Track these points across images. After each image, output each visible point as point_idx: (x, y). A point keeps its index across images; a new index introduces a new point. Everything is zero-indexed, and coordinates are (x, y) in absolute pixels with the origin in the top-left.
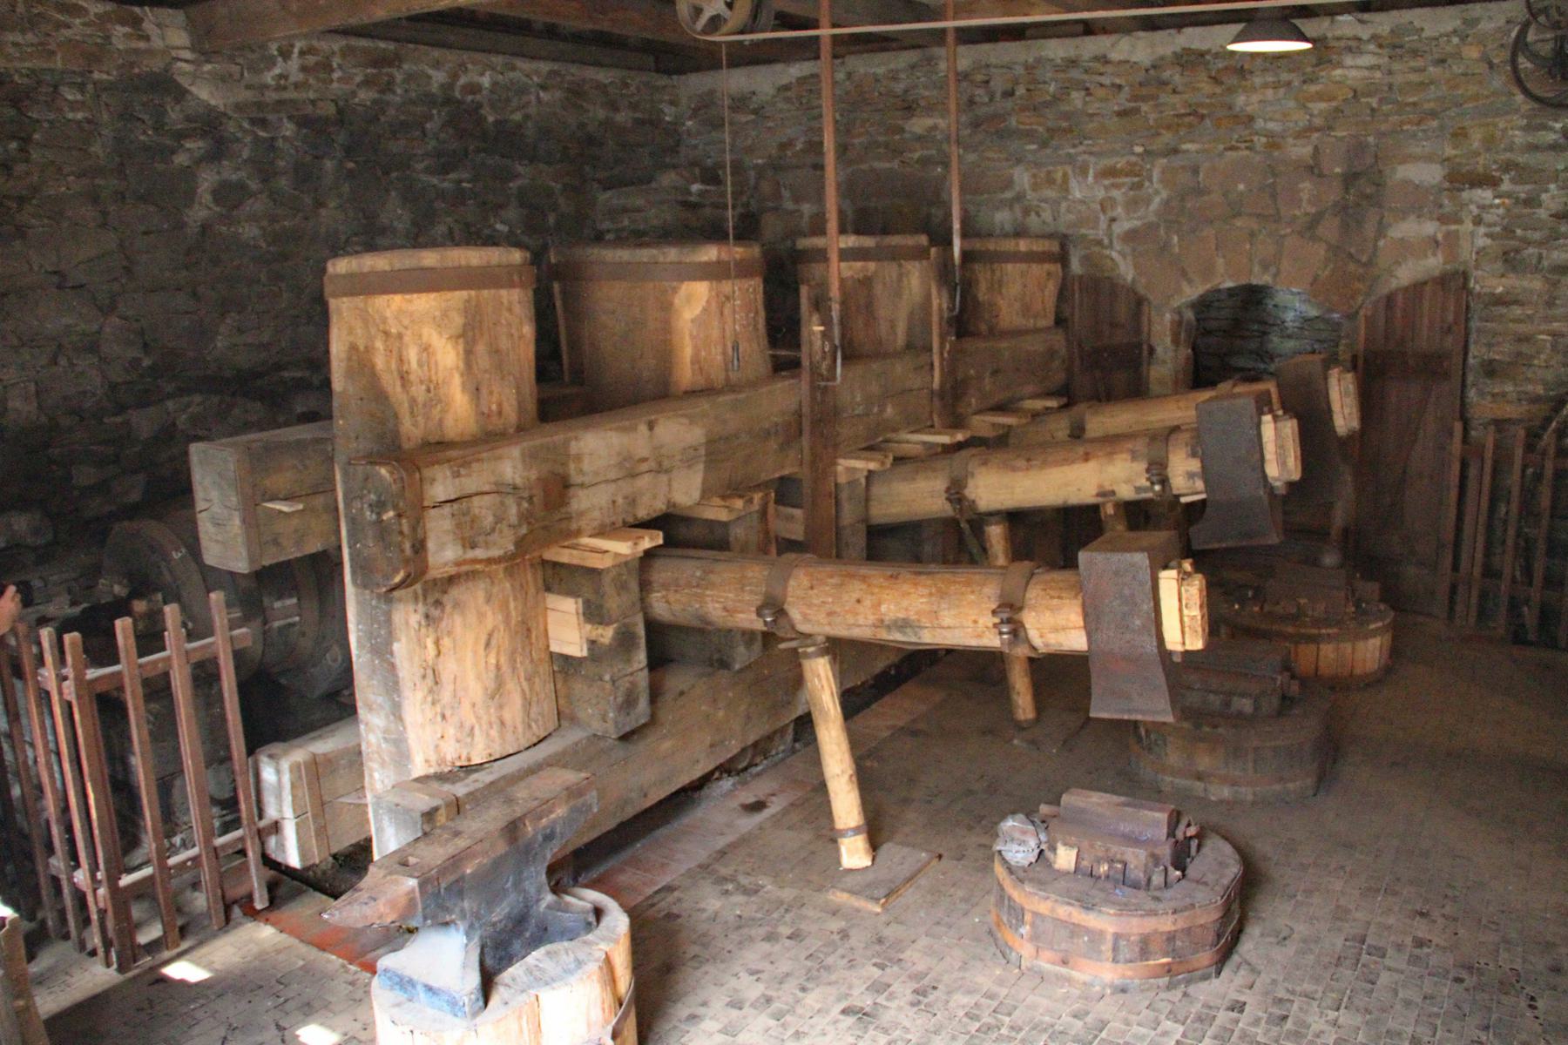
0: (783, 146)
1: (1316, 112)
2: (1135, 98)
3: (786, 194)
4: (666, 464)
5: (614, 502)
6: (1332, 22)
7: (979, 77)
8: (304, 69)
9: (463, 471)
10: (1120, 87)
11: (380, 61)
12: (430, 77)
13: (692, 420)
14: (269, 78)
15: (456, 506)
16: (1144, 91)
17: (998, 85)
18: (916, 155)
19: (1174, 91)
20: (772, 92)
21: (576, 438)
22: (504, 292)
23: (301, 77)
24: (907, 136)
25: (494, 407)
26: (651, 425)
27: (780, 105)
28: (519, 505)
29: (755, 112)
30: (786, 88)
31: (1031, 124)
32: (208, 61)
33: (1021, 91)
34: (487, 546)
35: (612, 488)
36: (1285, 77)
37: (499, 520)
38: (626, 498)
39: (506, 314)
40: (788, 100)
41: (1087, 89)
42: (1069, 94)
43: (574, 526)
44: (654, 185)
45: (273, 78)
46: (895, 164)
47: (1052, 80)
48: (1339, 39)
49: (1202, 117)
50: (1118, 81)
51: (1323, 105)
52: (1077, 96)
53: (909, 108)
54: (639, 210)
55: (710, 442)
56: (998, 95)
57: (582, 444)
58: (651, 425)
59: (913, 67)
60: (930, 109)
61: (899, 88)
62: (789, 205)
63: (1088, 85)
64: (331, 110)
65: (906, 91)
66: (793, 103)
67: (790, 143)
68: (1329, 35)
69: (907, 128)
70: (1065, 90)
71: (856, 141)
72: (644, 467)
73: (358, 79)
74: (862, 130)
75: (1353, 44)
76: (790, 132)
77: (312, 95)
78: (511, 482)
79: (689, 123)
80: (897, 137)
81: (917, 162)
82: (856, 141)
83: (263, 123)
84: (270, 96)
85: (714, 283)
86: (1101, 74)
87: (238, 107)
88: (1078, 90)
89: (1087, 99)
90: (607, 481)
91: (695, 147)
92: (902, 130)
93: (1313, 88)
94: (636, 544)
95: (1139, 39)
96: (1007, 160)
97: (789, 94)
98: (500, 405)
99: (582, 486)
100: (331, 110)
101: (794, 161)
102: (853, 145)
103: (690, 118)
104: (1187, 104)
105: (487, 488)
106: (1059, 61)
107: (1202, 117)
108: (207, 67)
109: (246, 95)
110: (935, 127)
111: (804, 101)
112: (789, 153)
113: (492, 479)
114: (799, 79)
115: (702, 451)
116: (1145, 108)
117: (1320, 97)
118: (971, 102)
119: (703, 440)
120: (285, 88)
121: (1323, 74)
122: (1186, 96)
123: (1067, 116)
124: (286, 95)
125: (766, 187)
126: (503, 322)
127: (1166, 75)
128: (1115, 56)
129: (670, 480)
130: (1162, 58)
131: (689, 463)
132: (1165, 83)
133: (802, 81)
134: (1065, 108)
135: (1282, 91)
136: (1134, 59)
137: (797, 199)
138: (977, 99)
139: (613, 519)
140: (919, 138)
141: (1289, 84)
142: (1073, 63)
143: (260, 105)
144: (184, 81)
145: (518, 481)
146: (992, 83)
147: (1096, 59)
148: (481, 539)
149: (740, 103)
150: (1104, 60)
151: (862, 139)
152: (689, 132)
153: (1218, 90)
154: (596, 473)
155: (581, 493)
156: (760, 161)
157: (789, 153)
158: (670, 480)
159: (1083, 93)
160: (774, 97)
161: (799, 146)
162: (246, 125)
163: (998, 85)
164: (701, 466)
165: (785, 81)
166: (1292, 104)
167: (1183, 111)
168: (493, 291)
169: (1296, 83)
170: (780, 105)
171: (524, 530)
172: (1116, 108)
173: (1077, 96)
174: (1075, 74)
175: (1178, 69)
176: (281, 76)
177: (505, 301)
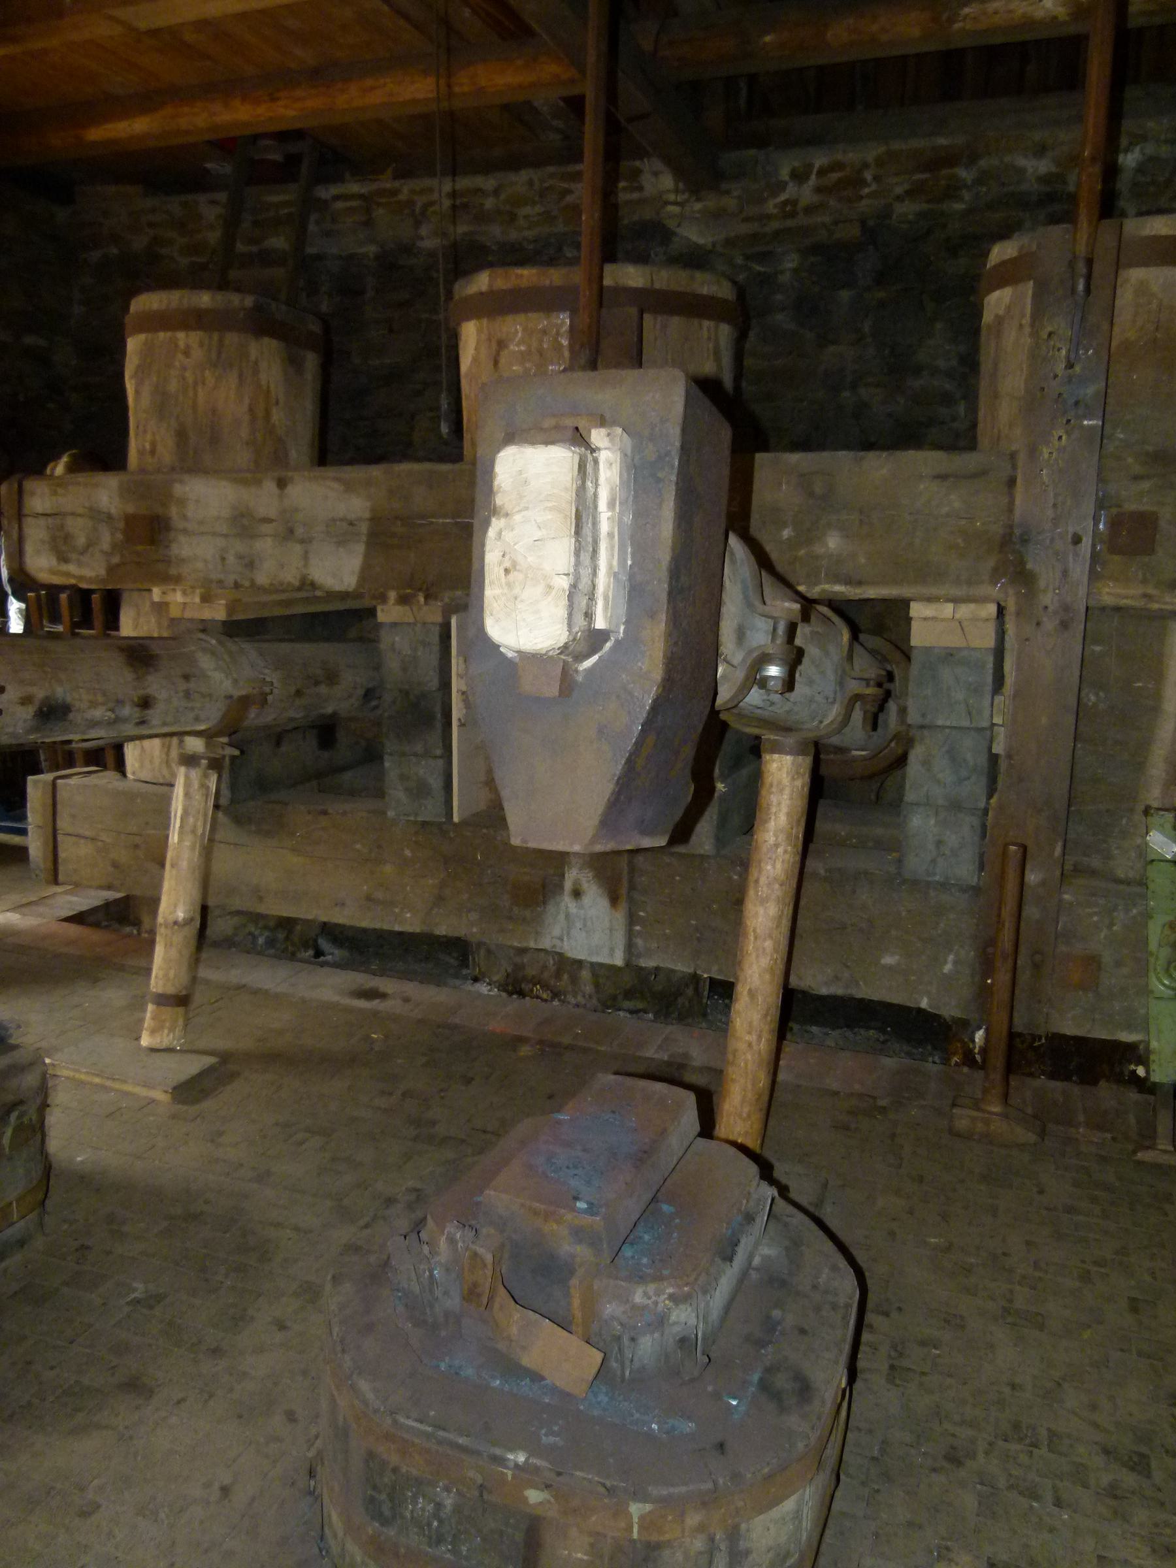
4: (300, 531)
5: (223, 559)
8: (818, 190)
9: (60, 490)
11: (949, 159)
12: (1022, 171)
13: (349, 487)
14: (771, 206)
15: (50, 520)
21: (182, 482)
22: (181, 335)
23: (816, 199)
25: (148, 446)
26: (282, 484)
28: (112, 534)
32: (698, 200)
34: (80, 564)
35: (221, 542)
37: (90, 545)
38: (240, 557)
39: (180, 356)
43: (173, 571)
45: (775, 206)
55: (374, 520)
57: (187, 489)
58: (282, 484)
64: (855, 231)
72: (266, 528)
73: (899, 190)
77: (827, 219)
78: (105, 510)
83: (763, 257)
84: (775, 225)
85: (485, 321)
87: (729, 242)
90: (214, 534)
94: (164, 593)
98: (153, 444)
99: (185, 531)
100: (855, 231)
105: (80, 511)
108: (698, 206)
109: (744, 229)
113: (87, 505)
115: (364, 528)
119: (367, 515)
120: (793, 215)
124: (790, 223)
126: (177, 364)
129: (306, 552)
131: (342, 541)
139: (222, 576)
143: (755, 237)
144: (671, 224)
145: (113, 511)
148: (74, 556)
154: (201, 523)
155: (182, 539)
158: (306, 552)
162: (739, 260)
164: (360, 548)
168: (169, 334)
171: (116, 560)
176: (785, 203)
177: (181, 344)
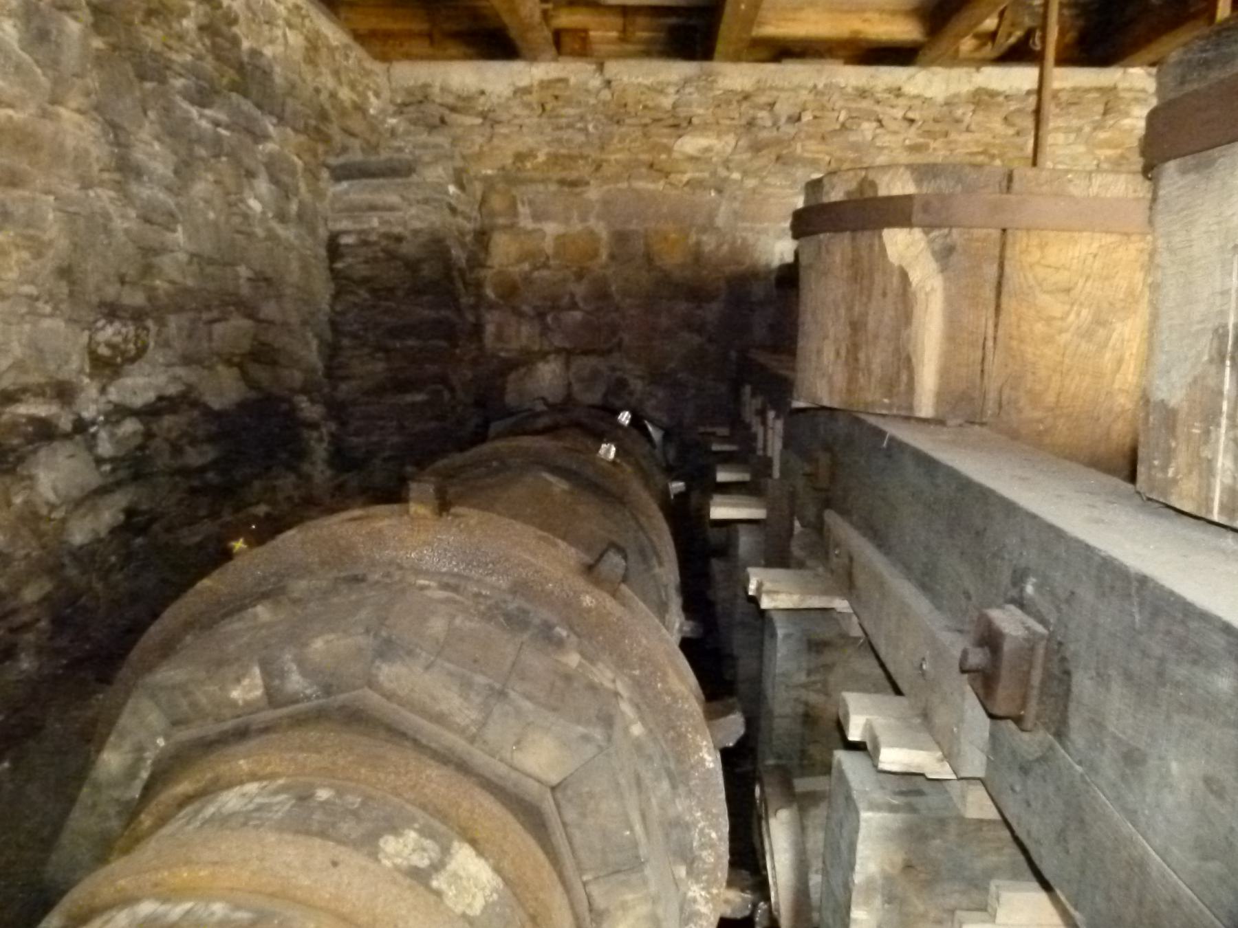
0: (520, 157)
1: (1102, 158)
2: (929, 133)
3: (523, 210)
6: (1125, 72)
7: (763, 99)
10: (912, 121)
16: (937, 127)
17: (784, 109)
18: (686, 178)
19: (968, 130)
20: (508, 92)
24: (676, 155)
27: (517, 110)
29: (484, 115)
30: (527, 90)
31: (818, 152)
33: (807, 117)
36: (1075, 123)
40: (528, 105)
41: (879, 121)
42: (859, 125)
44: (414, 178)
46: (661, 185)
47: (842, 108)
48: (1130, 90)
49: (993, 157)
50: (911, 115)
51: (1109, 152)
52: (868, 127)
53: (676, 126)
54: (392, 208)
56: (783, 119)
59: (686, 81)
60: (705, 128)
61: (667, 102)
62: (526, 223)
63: (881, 116)
65: (675, 106)
66: (533, 109)
67: (531, 154)
68: (1121, 86)
69: (676, 148)
70: (856, 118)
71: (613, 157)
74: (619, 146)
75: (1141, 95)
76: (529, 141)
79: (392, 121)
80: (663, 156)
81: (688, 183)
82: (613, 157)
86: (892, 107)
88: (868, 120)
89: (879, 131)
91: (400, 150)
92: (668, 150)
93: (1102, 135)
95: (934, 74)
96: (791, 187)
97: (527, 98)
101: (537, 175)
102: (607, 161)
103: (394, 115)
104: (977, 142)
106: (849, 90)
107: (993, 157)
110: (708, 149)
111: (548, 107)
112: (529, 165)
114: (542, 83)
116: (933, 145)
117: (1108, 144)
118: (751, 124)
121: (1111, 122)
122: (977, 136)
123: (855, 147)
125: (497, 202)
127: (959, 113)
128: (910, 89)
130: (957, 95)
132: (958, 121)
133: (545, 85)
134: (853, 138)
135: (1072, 137)
136: (928, 94)
137: (536, 217)
138: (759, 122)
140: (692, 159)
141: (1080, 129)
142: (863, 93)
146: (777, 107)
147: (889, 90)
149: (464, 103)
150: (898, 92)
151: (618, 156)
152: (393, 132)
153: (1011, 131)
156: (489, 172)
157: (529, 165)
159: (875, 124)
160: (508, 99)
161: (541, 158)
163: (784, 109)
165: (524, 82)
166: (1081, 149)
167: (975, 149)
169: (1087, 129)
170: (517, 110)
172: (907, 142)
173: (868, 127)
174: (865, 104)
175: (972, 107)
